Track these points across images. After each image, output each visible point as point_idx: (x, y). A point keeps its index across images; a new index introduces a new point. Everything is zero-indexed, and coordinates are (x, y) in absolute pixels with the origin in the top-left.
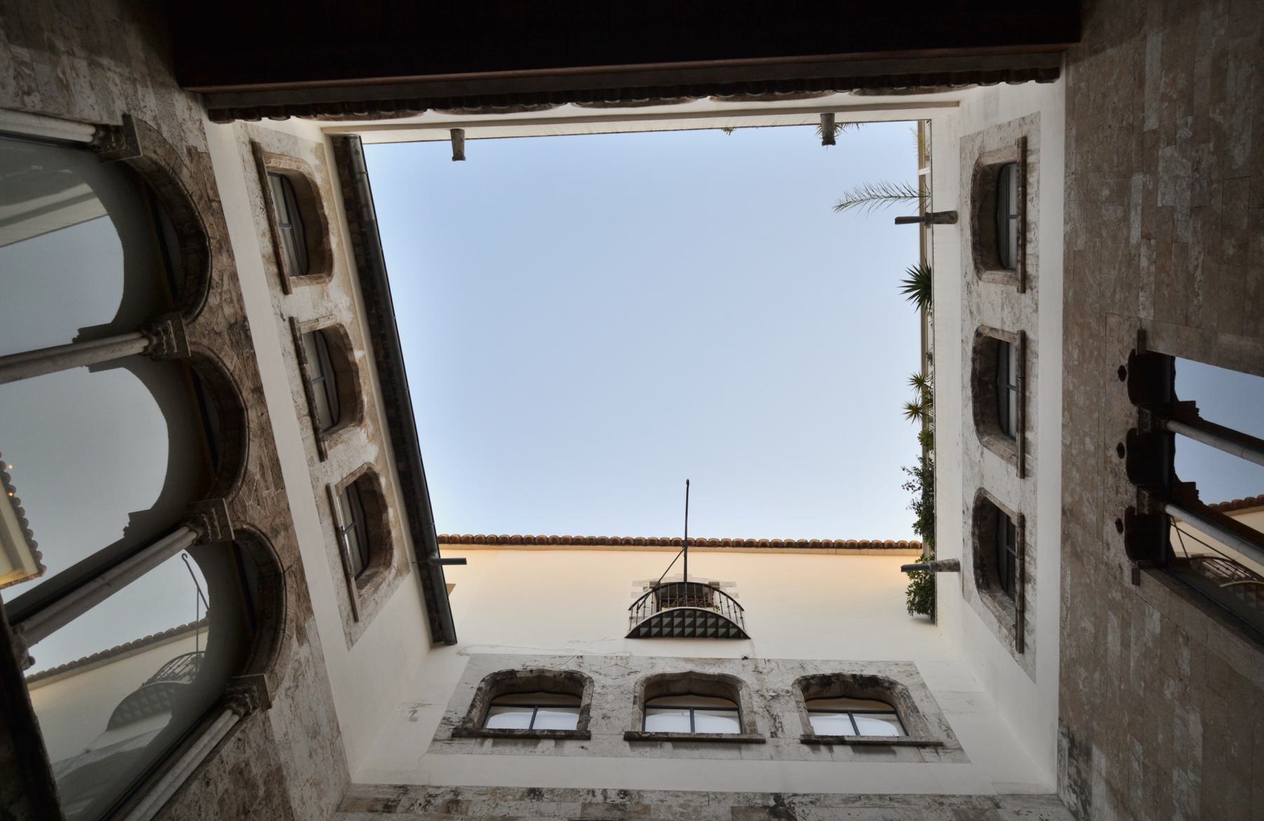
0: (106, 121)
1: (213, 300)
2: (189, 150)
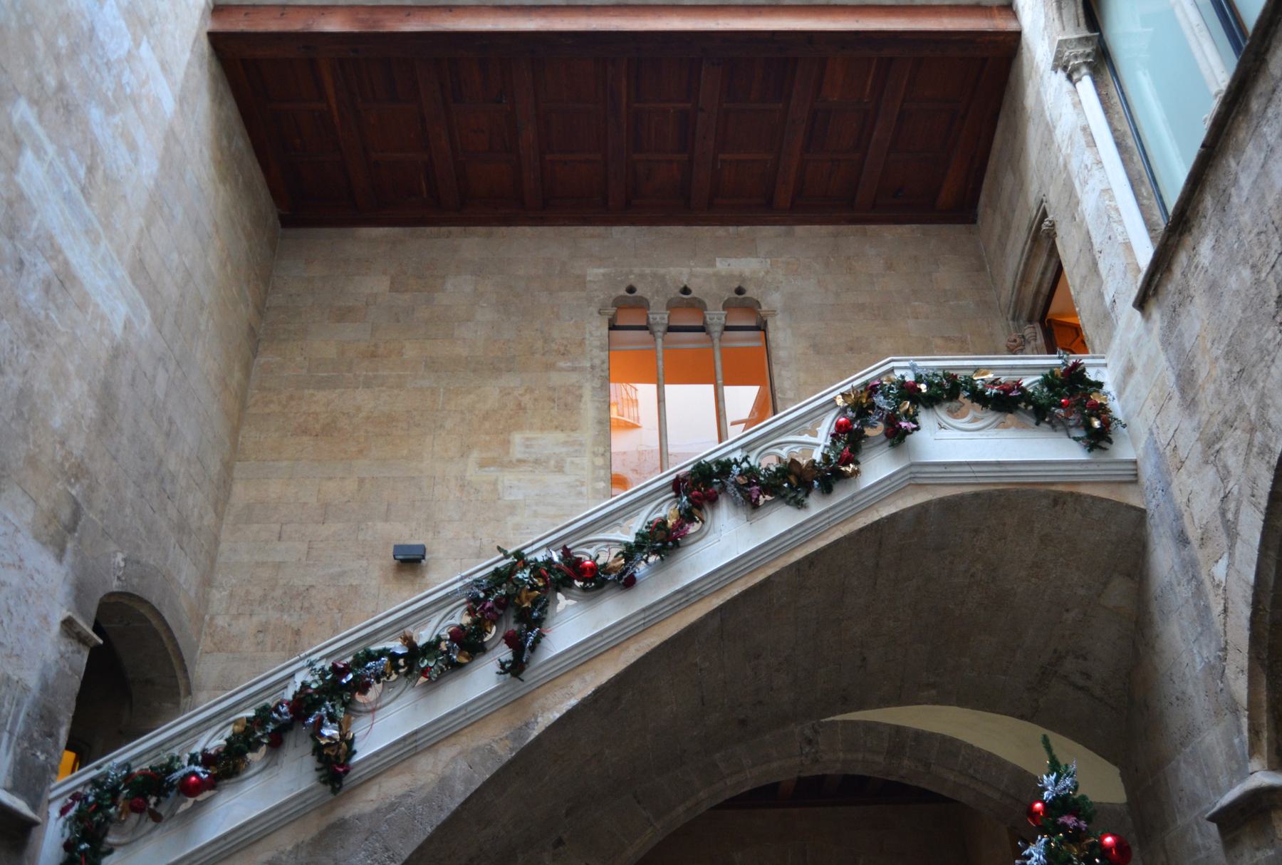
0: (1068, 85)
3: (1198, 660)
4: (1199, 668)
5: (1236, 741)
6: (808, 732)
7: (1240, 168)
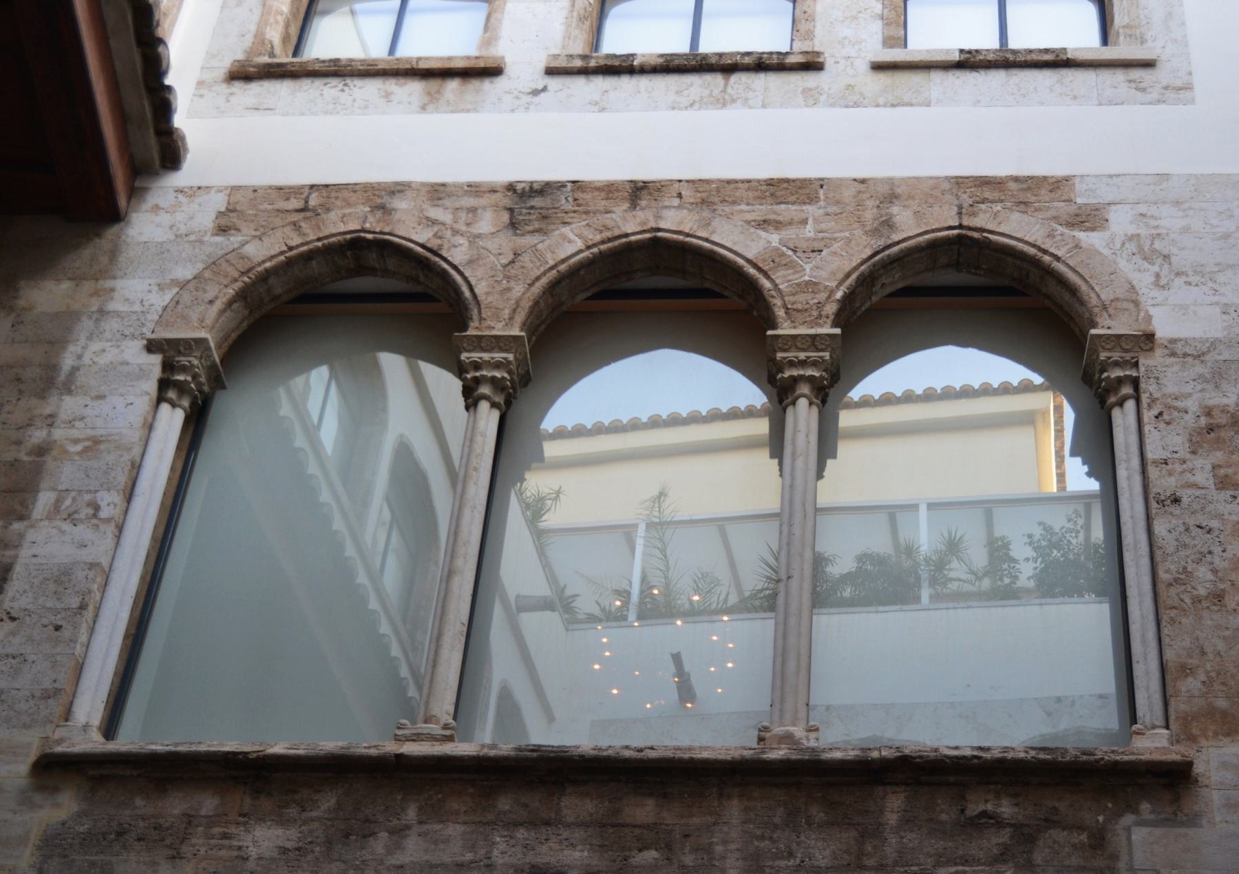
0: (151, 386)
1: (458, 253)
2: (222, 230)
7: (417, 829)
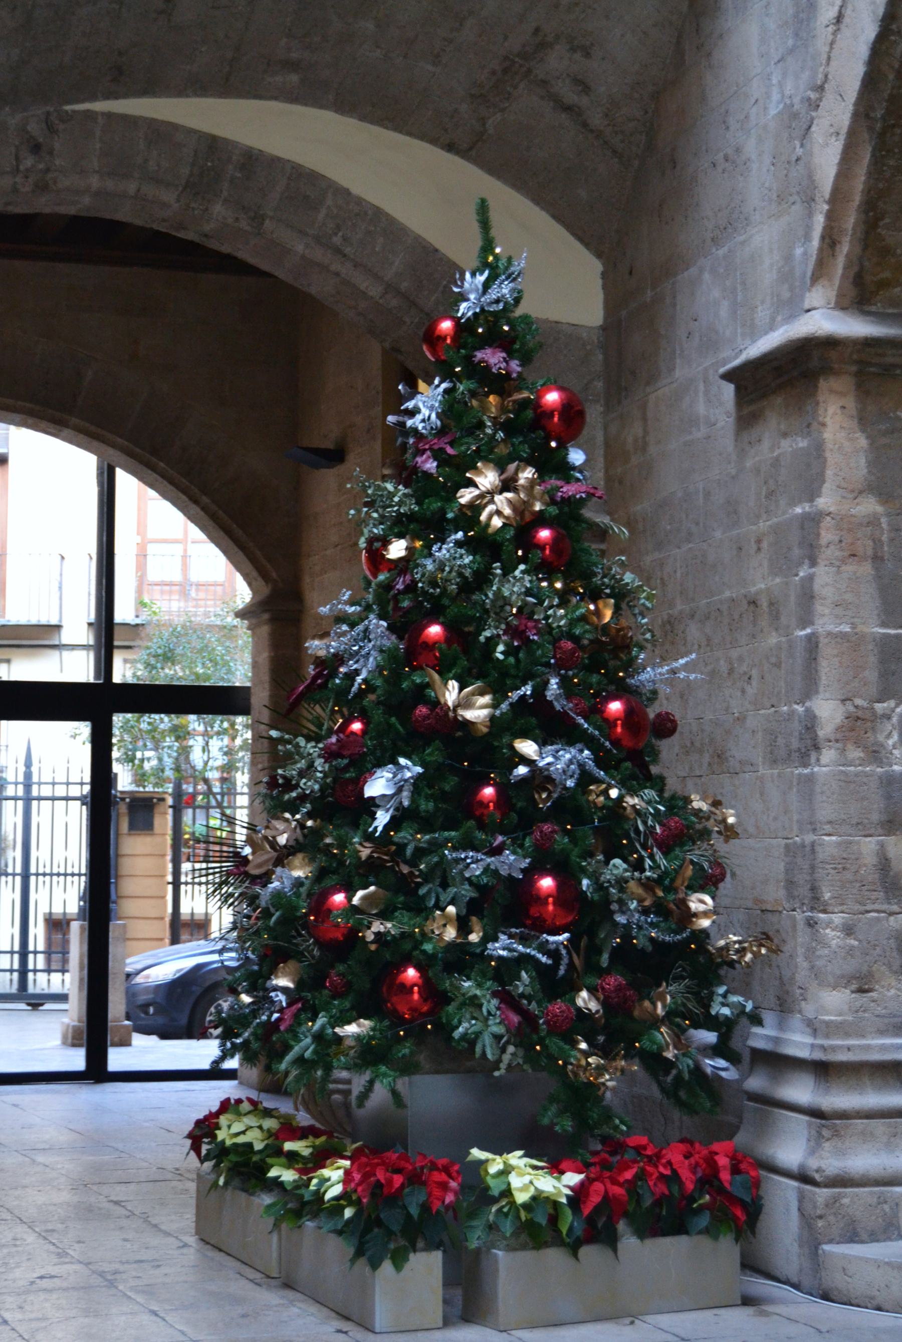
3: (775, 96)
4: (773, 112)
5: (799, 251)
6: (35, 128)
